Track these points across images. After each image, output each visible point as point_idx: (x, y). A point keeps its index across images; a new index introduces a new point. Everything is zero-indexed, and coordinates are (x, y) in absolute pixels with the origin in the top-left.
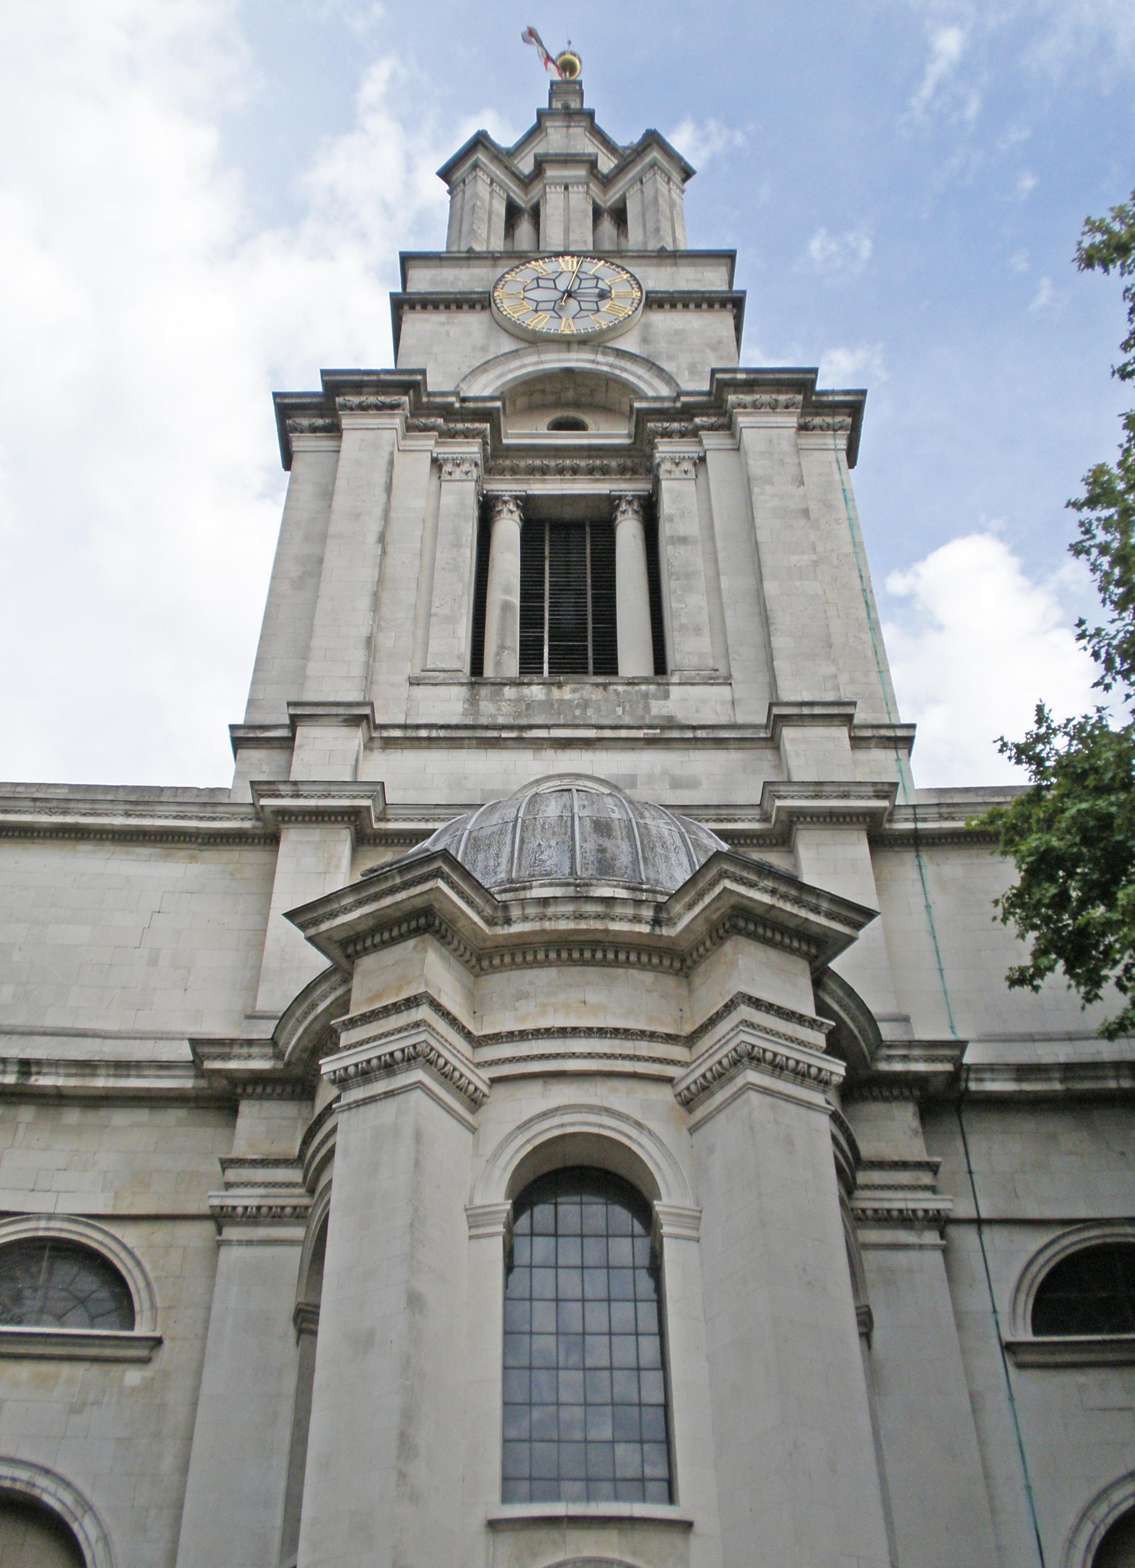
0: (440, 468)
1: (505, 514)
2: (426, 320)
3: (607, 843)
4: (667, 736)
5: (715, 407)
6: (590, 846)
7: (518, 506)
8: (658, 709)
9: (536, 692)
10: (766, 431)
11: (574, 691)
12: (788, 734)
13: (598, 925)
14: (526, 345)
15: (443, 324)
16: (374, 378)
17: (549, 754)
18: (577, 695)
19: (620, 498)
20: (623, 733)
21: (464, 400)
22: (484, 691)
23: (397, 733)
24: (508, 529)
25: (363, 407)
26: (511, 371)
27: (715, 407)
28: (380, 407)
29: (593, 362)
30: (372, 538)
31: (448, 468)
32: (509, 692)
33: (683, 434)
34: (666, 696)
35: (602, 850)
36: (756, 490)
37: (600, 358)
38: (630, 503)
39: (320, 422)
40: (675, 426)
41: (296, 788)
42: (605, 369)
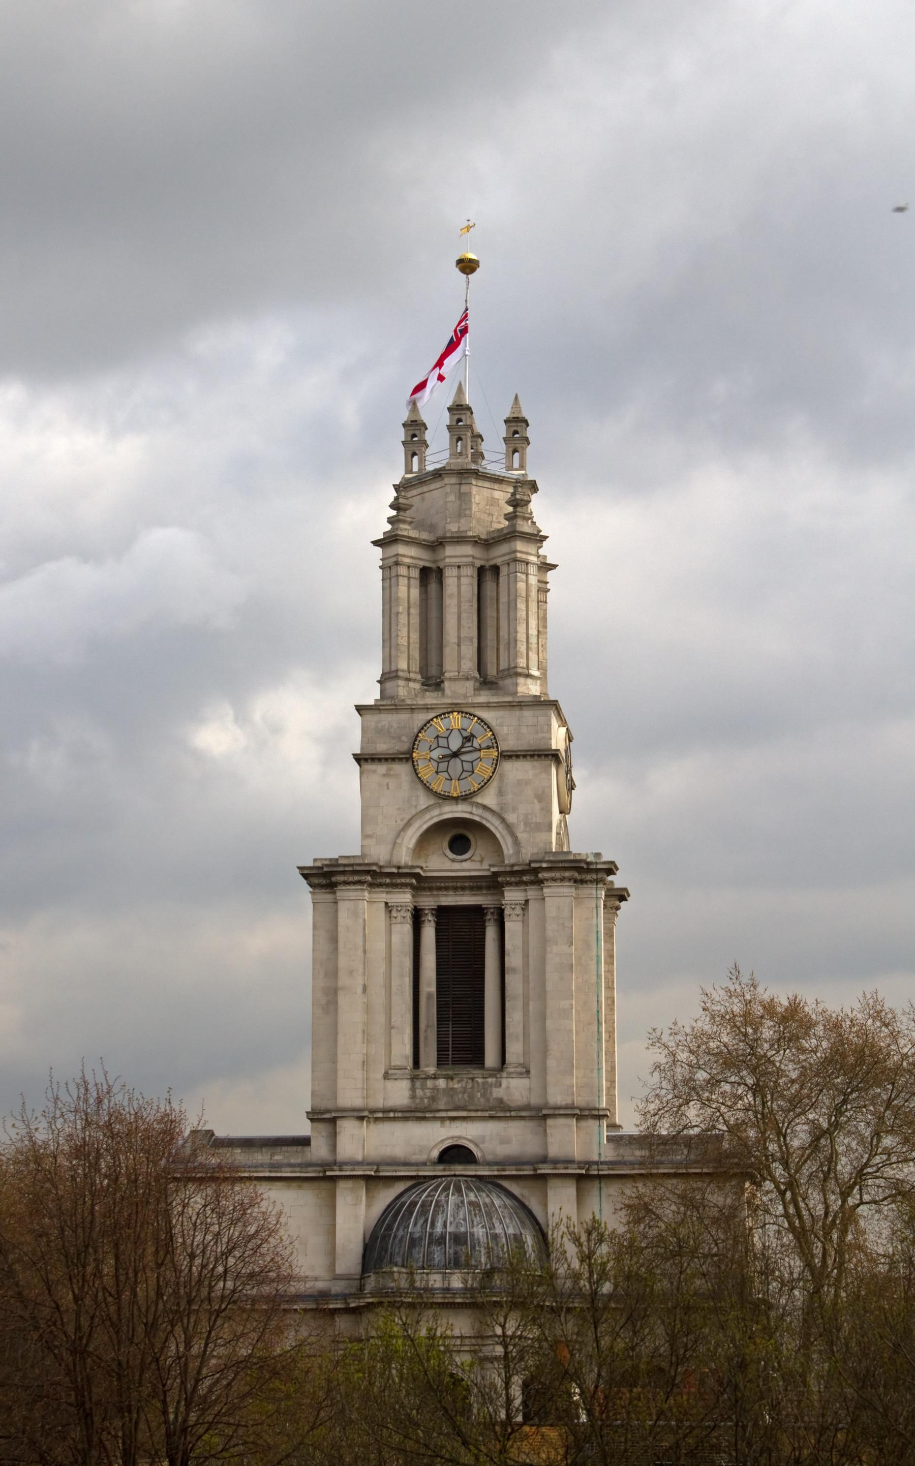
0: (390, 911)
1: (426, 924)
2: (375, 771)
3: (458, 1248)
4: (501, 1111)
5: (531, 875)
6: (452, 1251)
7: (433, 914)
8: (498, 1093)
9: (442, 1083)
10: (558, 898)
11: (459, 1082)
12: (550, 1122)
13: (451, 1300)
14: (432, 801)
15: (384, 775)
16: (350, 869)
17: (447, 1123)
18: (460, 1085)
19: (487, 908)
20: (479, 1114)
21: (399, 868)
22: (418, 1084)
23: (380, 1115)
24: (429, 933)
25: (346, 883)
26: (425, 823)
27: (531, 875)
28: (355, 883)
29: (471, 813)
30: (359, 990)
31: (394, 914)
32: (430, 1083)
33: (517, 884)
34: (500, 1085)
35: (456, 1253)
36: (548, 949)
37: (475, 810)
38: (492, 913)
39: (324, 882)
40: (513, 879)
41: (341, 1165)
42: (477, 819)
